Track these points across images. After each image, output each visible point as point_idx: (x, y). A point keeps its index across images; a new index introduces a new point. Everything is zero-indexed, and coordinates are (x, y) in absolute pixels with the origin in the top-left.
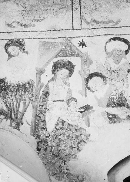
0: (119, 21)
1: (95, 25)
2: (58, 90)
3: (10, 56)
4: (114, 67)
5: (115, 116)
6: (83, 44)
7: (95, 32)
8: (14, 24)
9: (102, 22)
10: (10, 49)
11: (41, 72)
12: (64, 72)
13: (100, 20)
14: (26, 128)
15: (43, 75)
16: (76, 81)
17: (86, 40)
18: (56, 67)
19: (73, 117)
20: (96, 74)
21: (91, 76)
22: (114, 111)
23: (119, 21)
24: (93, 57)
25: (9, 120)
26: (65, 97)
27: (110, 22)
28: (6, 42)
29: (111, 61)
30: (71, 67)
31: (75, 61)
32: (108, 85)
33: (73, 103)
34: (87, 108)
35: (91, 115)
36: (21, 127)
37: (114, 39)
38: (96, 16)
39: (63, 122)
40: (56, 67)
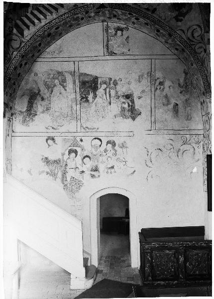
0: (98, 129)
1: (87, 130)
2: (71, 164)
3: (49, 145)
4: (95, 153)
5: (93, 175)
6: (81, 140)
7: (87, 134)
8: (49, 128)
9: (91, 129)
10: (49, 141)
11: (63, 154)
12: (73, 155)
13: (89, 127)
14: (59, 180)
15: (65, 156)
16: (79, 158)
17: (83, 138)
18: (70, 152)
19: (77, 175)
20: (87, 156)
21: (84, 158)
22: (93, 173)
23: (98, 129)
24: (85, 148)
25: (51, 177)
26: (74, 167)
27: (94, 129)
28: (46, 138)
29: (93, 150)
30: (76, 152)
31: (78, 149)
32: (91, 162)
33: (77, 169)
34: (83, 172)
35: (84, 175)
36: (57, 180)
37: (95, 138)
38: (89, 125)
39: (74, 178)
40: (70, 152)
